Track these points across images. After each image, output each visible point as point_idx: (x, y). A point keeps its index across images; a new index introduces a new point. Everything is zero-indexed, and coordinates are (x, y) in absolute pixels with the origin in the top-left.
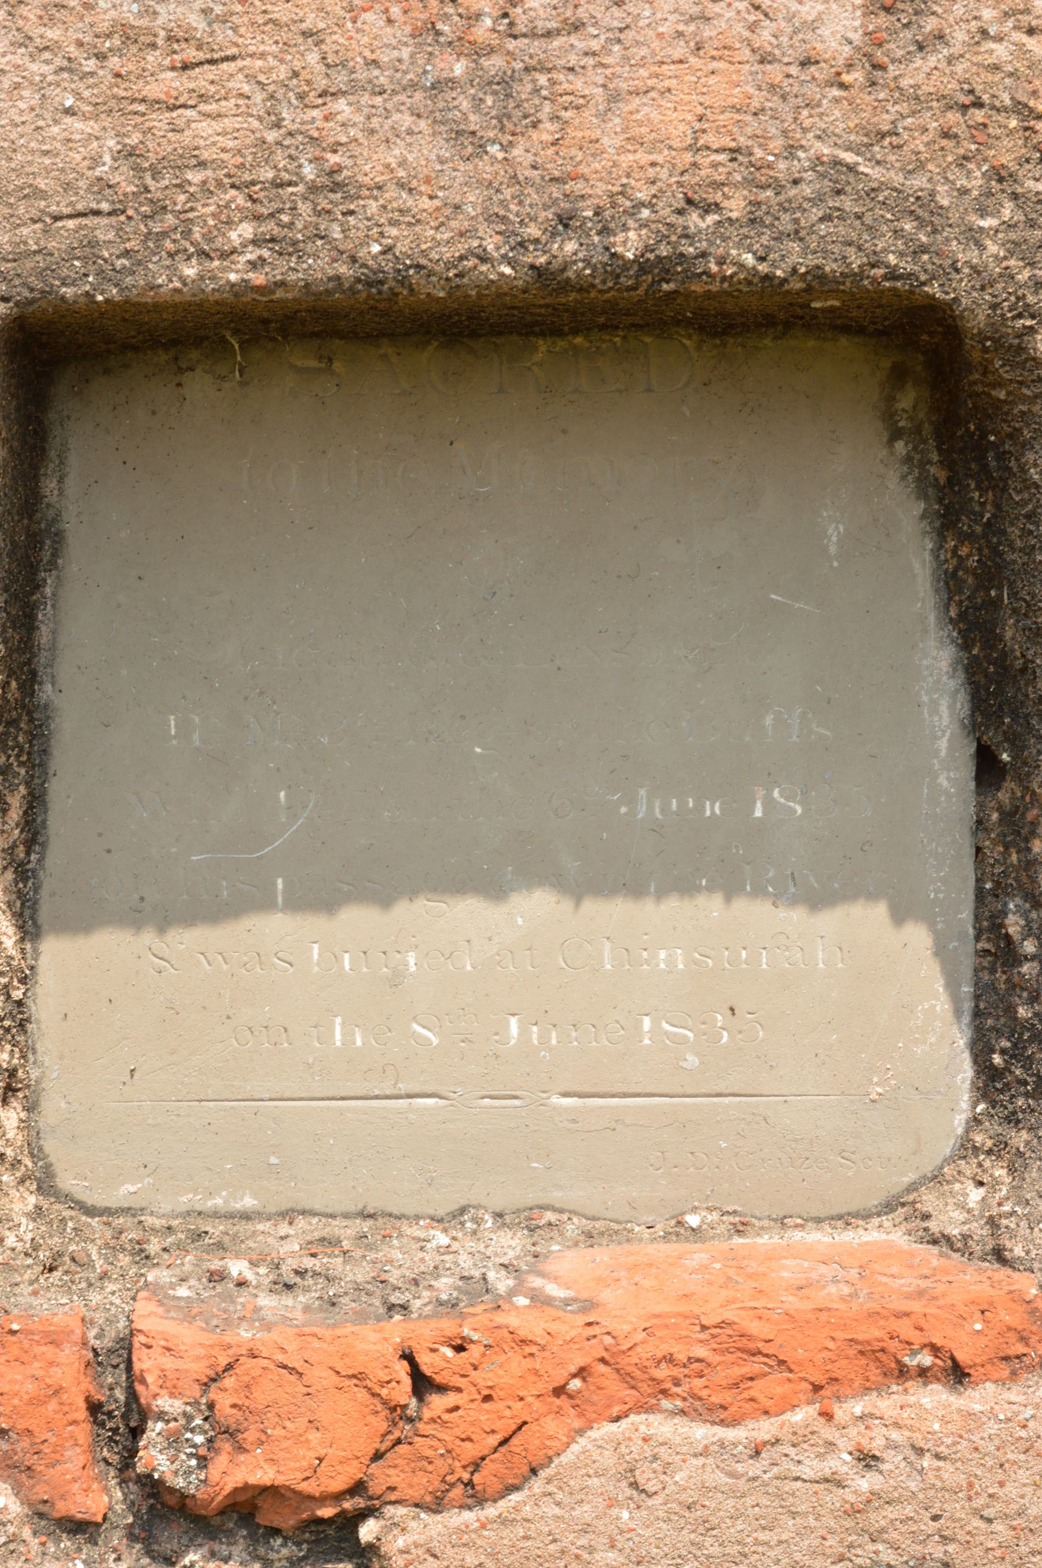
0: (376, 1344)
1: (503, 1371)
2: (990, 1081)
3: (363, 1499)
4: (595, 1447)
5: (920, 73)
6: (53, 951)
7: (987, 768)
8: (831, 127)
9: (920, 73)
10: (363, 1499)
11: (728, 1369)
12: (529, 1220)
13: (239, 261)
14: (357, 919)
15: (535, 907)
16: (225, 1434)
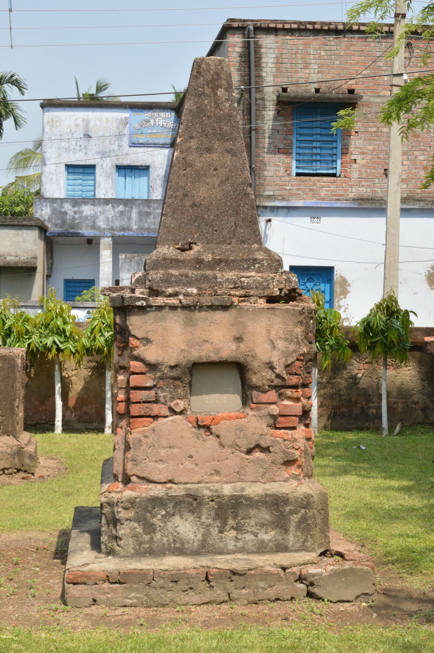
0: (211, 417)
1: (218, 418)
2: (243, 404)
3: (210, 425)
4: (222, 422)
5: (239, 351)
6: (192, 397)
7: (242, 387)
8: (234, 354)
9: (239, 351)
10: (210, 425)
11: (229, 418)
12: (218, 412)
13: (205, 360)
14: (208, 395)
15: (218, 395)
16: (203, 422)
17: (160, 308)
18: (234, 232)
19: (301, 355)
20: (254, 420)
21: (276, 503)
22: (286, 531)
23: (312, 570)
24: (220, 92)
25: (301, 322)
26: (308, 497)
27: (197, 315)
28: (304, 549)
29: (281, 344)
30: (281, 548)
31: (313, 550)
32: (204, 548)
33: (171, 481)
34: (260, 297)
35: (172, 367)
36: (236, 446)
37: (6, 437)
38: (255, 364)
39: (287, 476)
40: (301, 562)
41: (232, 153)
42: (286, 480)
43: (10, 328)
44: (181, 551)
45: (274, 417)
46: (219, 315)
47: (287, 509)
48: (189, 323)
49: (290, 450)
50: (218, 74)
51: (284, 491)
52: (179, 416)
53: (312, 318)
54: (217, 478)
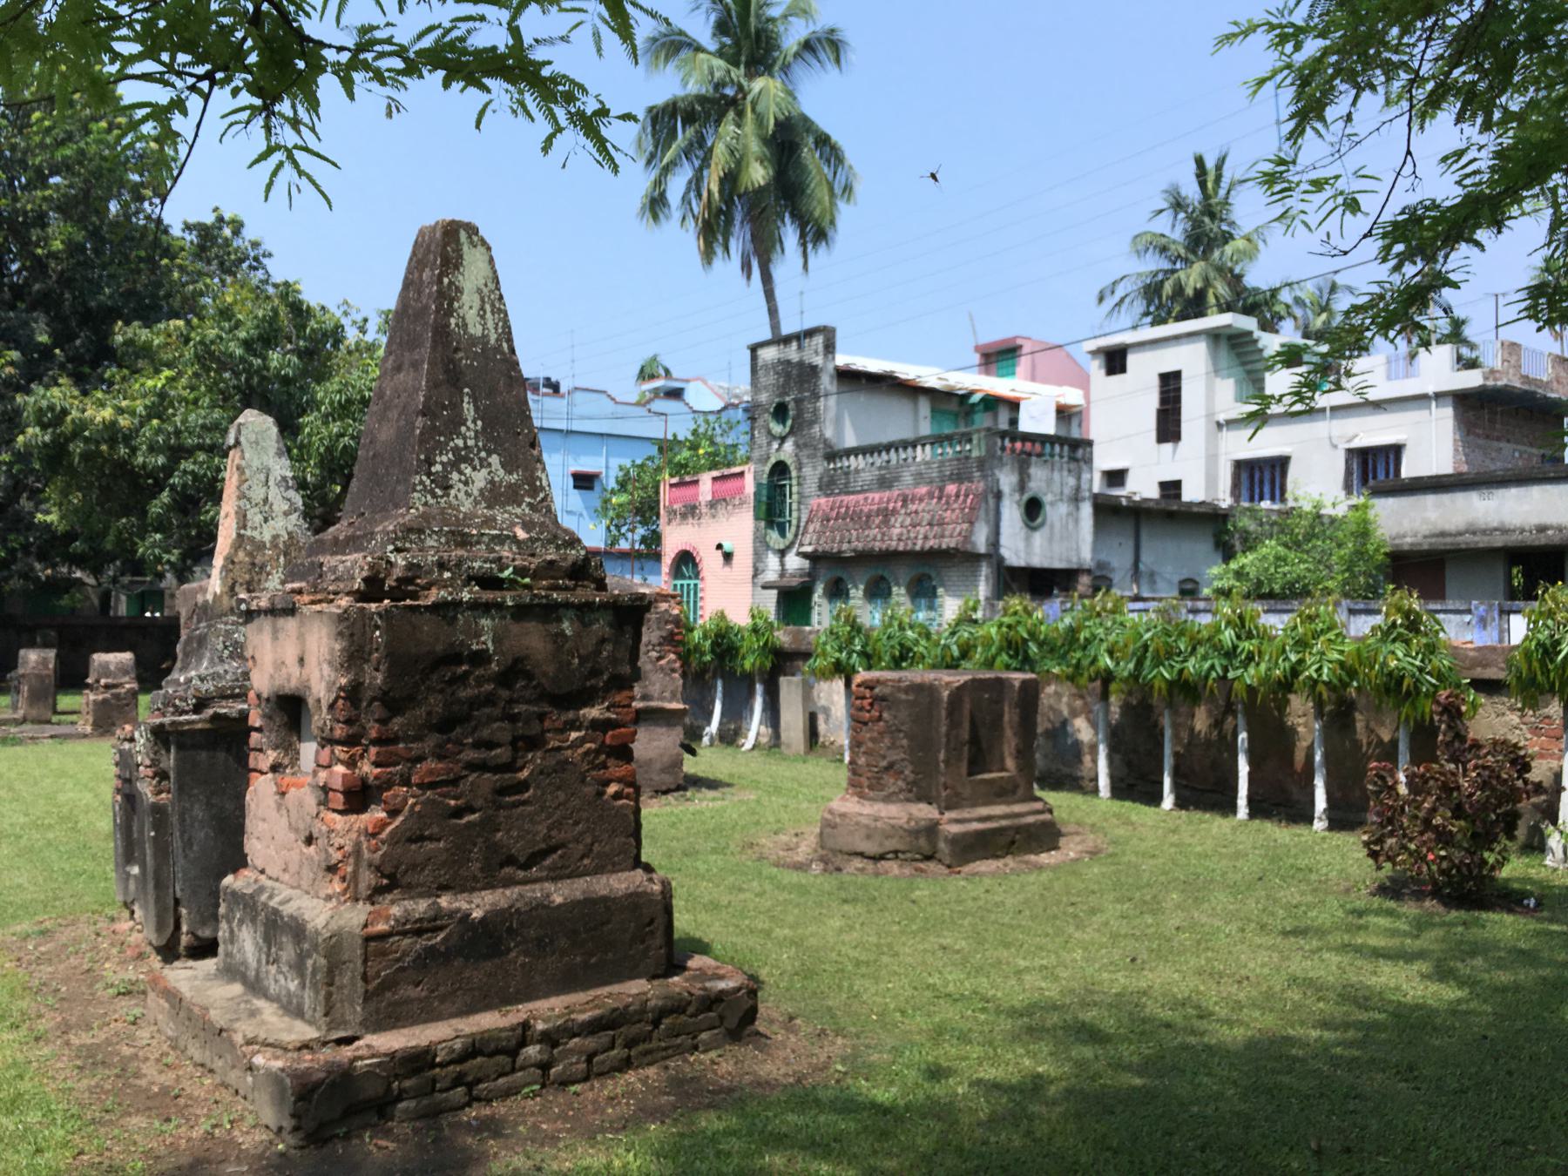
17: (259, 612)
18: (393, 492)
19: (341, 688)
20: (306, 789)
21: (297, 929)
22: (304, 987)
23: (259, 1060)
24: (426, 275)
25: (340, 634)
26: (317, 933)
27: (281, 622)
28: (310, 1023)
29: (326, 669)
30: (298, 1013)
31: (319, 1029)
32: (255, 987)
33: (262, 872)
34: (348, 594)
35: (268, 700)
36: (297, 830)
37: (923, 806)
38: (311, 701)
39: (330, 891)
40: (271, 1040)
41: (416, 365)
42: (329, 898)
43: (1146, 647)
44: (244, 980)
45: (325, 789)
46: (290, 624)
47: (306, 946)
48: (275, 633)
49: (331, 850)
50: (429, 246)
51: (306, 917)
52: (270, 775)
53: (377, 627)
54: (286, 877)
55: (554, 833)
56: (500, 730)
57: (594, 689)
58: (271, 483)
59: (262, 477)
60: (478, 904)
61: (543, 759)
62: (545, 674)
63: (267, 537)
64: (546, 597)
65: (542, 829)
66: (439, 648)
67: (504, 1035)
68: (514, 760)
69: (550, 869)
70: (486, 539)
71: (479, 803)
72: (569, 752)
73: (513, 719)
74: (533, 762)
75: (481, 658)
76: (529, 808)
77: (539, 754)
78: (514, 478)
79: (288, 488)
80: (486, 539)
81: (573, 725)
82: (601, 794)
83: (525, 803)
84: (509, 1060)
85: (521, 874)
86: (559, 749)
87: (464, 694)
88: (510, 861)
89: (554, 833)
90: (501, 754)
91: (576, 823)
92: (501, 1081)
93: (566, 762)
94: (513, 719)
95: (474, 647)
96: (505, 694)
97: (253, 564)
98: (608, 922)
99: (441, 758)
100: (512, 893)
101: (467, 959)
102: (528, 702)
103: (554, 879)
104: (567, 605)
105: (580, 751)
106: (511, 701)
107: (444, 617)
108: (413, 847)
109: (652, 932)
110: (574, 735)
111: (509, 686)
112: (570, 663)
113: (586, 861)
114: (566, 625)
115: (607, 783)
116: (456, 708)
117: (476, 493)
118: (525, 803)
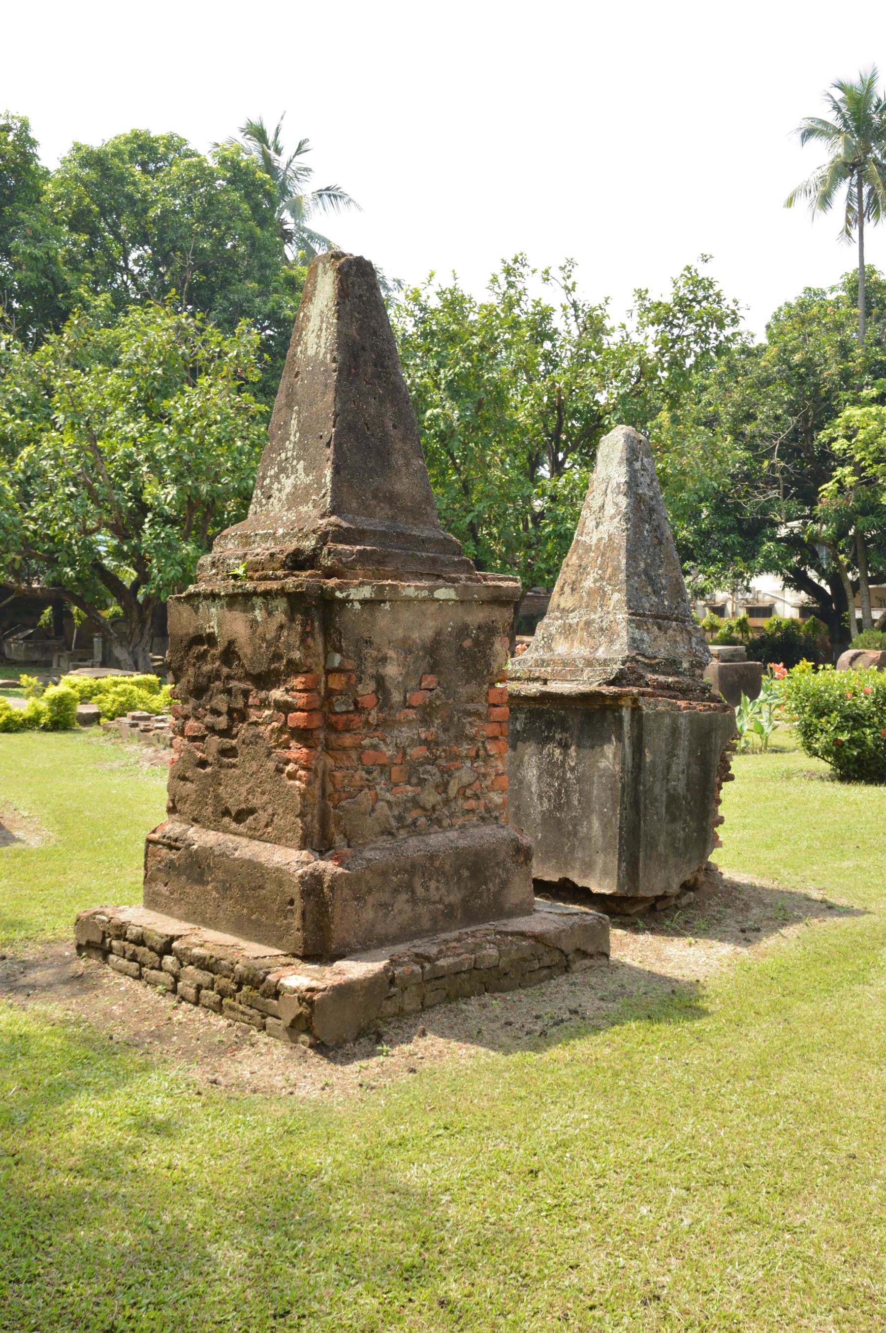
55: (250, 797)
56: (221, 702)
57: (277, 672)
58: (609, 491)
59: (603, 487)
60: (202, 838)
61: (247, 730)
62: (246, 656)
63: (594, 541)
64: (241, 586)
65: (243, 790)
66: (191, 631)
67: (156, 937)
68: (230, 728)
69: (250, 829)
70: (258, 538)
71: (210, 759)
72: (263, 727)
73: (229, 692)
74: (243, 730)
75: (211, 639)
76: (237, 772)
77: (245, 725)
78: (308, 480)
79: (619, 493)
80: (258, 538)
81: (264, 704)
82: (280, 771)
83: (234, 766)
84: (157, 958)
85: (234, 825)
86: (256, 724)
87: (206, 668)
88: (226, 812)
89: (250, 797)
90: (222, 722)
91: (263, 793)
92: (154, 972)
93: (258, 736)
94: (229, 692)
95: (208, 631)
96: (225, 670)
97: (580, 566)
98: (261, 887)
99: (197, 718)
100: (222, 836)
101: (188, 878)
102: (239, 679)
103: (252, 838)
104: (255, 593)
105: (270, 727)
106: (229, 677)
107: (193, 606)
108: (182, 783)
109: (291, 910)
110: (267, 712)
111: (229, 665)
112: (261, 647)
113: (270, 829)
114: (257, 612)
115: (287, 762)
116: (201, 679)
117: (284, 498)
118: (234, 766)
